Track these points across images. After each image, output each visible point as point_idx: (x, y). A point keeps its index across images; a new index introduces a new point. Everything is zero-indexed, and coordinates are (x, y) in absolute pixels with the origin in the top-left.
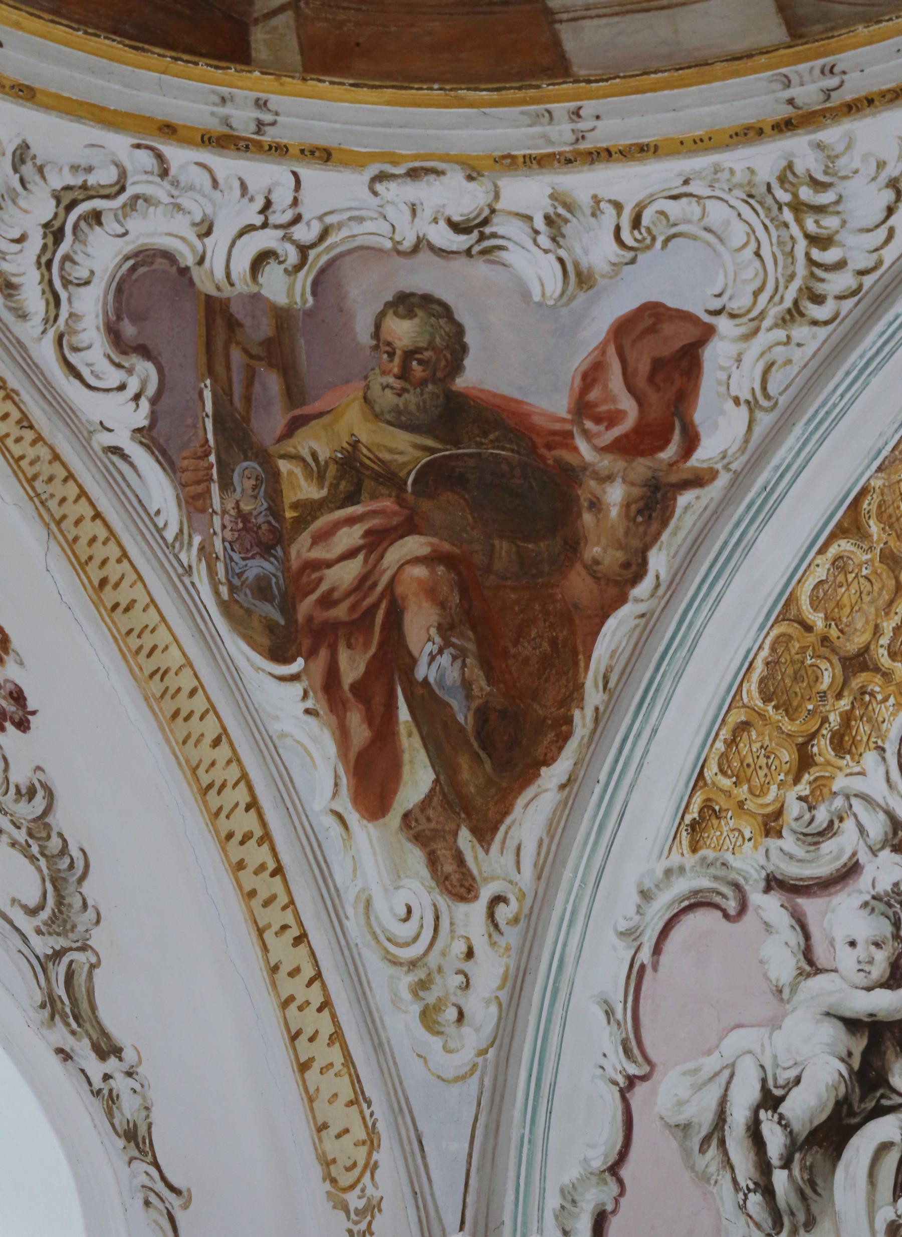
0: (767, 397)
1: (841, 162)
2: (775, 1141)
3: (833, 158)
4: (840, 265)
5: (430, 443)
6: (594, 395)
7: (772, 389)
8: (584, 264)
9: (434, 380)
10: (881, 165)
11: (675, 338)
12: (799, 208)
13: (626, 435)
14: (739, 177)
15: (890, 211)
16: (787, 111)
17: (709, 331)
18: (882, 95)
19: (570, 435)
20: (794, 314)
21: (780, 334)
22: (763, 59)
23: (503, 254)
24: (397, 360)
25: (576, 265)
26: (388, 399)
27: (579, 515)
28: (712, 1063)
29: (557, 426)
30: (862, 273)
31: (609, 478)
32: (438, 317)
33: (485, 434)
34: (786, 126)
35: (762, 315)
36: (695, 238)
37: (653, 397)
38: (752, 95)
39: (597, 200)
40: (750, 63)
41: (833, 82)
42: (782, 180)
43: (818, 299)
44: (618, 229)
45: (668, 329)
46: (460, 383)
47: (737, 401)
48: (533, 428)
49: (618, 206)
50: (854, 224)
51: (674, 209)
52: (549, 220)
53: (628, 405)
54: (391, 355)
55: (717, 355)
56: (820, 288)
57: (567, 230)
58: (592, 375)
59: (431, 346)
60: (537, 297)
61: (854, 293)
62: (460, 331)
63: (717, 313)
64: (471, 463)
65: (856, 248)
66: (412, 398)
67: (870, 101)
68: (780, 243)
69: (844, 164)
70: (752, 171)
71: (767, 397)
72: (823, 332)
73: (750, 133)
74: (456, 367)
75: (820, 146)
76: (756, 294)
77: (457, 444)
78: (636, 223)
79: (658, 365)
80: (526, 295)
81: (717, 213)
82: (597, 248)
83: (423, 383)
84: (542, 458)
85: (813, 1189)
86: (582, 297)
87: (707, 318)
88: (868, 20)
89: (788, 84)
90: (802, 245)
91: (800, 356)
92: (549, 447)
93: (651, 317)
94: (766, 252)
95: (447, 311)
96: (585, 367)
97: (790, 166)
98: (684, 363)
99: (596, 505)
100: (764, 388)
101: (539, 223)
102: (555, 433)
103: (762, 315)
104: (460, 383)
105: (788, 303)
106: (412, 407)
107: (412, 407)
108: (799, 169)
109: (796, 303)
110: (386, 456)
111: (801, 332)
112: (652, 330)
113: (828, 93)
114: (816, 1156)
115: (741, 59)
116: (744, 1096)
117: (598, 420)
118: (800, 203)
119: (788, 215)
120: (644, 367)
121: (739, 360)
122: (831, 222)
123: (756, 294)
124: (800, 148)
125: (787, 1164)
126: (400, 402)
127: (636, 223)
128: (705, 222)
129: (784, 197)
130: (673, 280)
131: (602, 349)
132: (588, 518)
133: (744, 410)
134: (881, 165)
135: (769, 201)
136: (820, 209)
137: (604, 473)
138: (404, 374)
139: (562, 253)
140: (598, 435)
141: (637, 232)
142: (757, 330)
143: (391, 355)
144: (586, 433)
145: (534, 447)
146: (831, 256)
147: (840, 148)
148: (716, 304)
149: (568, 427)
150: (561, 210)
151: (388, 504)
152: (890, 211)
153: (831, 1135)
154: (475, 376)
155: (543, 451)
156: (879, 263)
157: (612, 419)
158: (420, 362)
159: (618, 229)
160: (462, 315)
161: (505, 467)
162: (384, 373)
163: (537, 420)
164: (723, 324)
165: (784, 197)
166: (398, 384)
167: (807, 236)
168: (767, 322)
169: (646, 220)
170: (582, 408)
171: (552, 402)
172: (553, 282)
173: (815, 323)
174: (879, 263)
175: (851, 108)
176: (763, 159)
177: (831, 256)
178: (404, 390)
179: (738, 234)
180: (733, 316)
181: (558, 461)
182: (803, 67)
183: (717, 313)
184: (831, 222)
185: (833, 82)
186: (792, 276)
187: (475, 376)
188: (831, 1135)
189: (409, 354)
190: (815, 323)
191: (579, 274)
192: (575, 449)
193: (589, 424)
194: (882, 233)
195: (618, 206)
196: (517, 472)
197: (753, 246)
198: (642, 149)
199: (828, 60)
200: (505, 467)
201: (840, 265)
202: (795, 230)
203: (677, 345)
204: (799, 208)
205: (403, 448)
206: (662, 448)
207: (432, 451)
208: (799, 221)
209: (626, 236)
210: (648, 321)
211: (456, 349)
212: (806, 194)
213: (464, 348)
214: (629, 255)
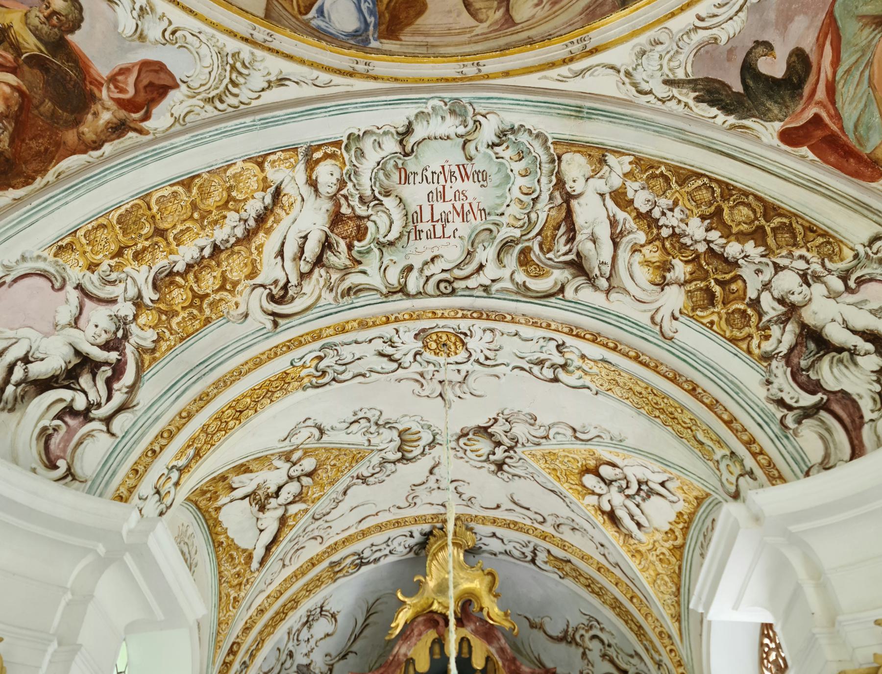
0: (184, 120)
1: (256, 63)
2: (18, 374)
3: (255, 61)
4: (236, 96)
5: (43, 49)
6: (120, 78)
7: (187, 119)
8: (145, 33)
9: (59, 28)
10: (269, 74)
11: (163, 80)
12: (233, 68)
13: (124, 100)
14: (218, 44)
15: (263, 90)
16: (248, 36)
17: (177, 86)
18: (283, 53)
19: (102, 85)
20: (211, 100)
21: (202, 104)
22: (251, 16)
23: (116, 6)
24: (49, 11)
25: (142, 31)
26: (36, 22)
27: (87, 114)
28: (10, 333)
29: (99, 79)
30: (241, 103)
31: (108, 109)
32: (76, 8)
33: (68, 62)
34: (246, 40)
35: (199, 93)
36: (191, 53)
37: (142, 94)
38: (242, 25)
39: (164, 15)
40: (246, 14)
41: (269, 39)
42: (233, 55)
43: (222, 101)
44: (165, 30)
45: (162, 75)
46: (69, 37)
47: (172, 115)
48: (89, 72)
49: (170, 23)
50: (249, 86)
51: (190, 38)
52: (141, 8)
53: (131, 91)
54: (47, 7)
55: (174, 96)
56: (224, 98)
57: (146, 16)
58: (124, 71)
59: (66, 16)
60: (120, 30)
61: (235, 107)
62: (82, 19)
63: (184, 82)
64: (56, 67)
65: (245, 94)
66: (46, 28)
67: (278, 52)
68: (220, 75)
69: (257, 65)
70: (225, 45)
71: (184, 120)
72: (216, 113)
73: (233, 34)
74: (72, 31)
75: (252, 54)
76: (201, 85)
77: (53, 57)
78: (174, 33)
79: (151, 84)
80: (116, 27)
81: (204, 50)
82: (154, 31)
83: (54, 26)
84: (86, 85)
85: (21, 400)
86: (137, 43)
87: (179, 81)
88: (292, 30)
89: (254, 29)
90: (227, 80)
91: (203, 115)
92: (91, 83)
93: (159, 67)
94: (213, 74)
95: (81, 9)
96: (123, 66)
97: (239, 53)
98: (161, 90)
99: (96, 114)
100: (184, 117)
101: (137, 7)
102: (96, 80)
103: (199, 93)
104: (69, 37)
105: (210, 96)
106: (44, 32)
107: (44, 32)
108: (241, 56)
109: (213, 97)
110: (21, 40)
111: (209, 107)
112: (156, 71)
113: (265, 41)
114: (31, 389)
115: (243, 11)
116: (16, 352)
117: (116, 87)
118: (236, 68)
119: (228, 68)
120: (145, 82)
121: (181, 102)
122: (241, 80)
123: (201, 85)
124: (246, 50)
125: (17, 385)
126: (40, 26)
127: (174, 33)
128: (198, 50)
129: (231, 61)
130: (176, 62)
131: (134, 65)
132: (90, 117)
133: (173, 119)
134: (269, 74)
135: (225, 59)
136: (240, 73)
137: (106, 106)
138: (48, 18)
139: (139, 23)
140: (113, 92)
141: (171, 36)
142: (194, 97)
143: (47, 7)
144: (108, 88)
145: (85, 79)
146: (235, 90)
147: (258, 59)
148: (185, 79)
149: (103, 82)
150: (148, 8)
151: (10, 57)
152: (263, 90)
153: (43, 385)
154: (75, 39)
155: (88, 83)
156: (249, 104)
157: (122, 91)
158: (58, 18)
159: (165, 30)
160: (86, 14)
161: (68, 78)
162: (40, 11)
163: (92, 71)
164: (183, 87)
165: (231, 61)
166: (43, 19)
167: (231, 79)
168: (199, 97)
169: (178, 34)
170: (113, 79)
171: (102, 68)
172: (129, 30)
173: (216, 108)
174: (249, 104)
175: (270, 50)
176: (232, 45)
177: (235, 90)
178: (44, 23)
179: (207, 62)
180: (188, 87)
181: (91, 92)
182: (263, 29)
183: (184, 82)
184: (241, 80)
185: (269, 39)
186: (217, 88)
187: (75, 39)
188: (43, 385)
189: (55, 13)
190: (216, 108)
191: (141, 34)
192: (101, 91)
193: (112, 86)
194: (257, 95)
195: (170, 23)
196: (72, 83)
197: (210, 69)
198: (191, 11)
199: (272, 32)
200: (68, 78)
201: (236, 96)
202: (228, 74)
203: (162, 82)
204: (233, 68)
205: (31, 44)
206: (134, 112)
207: (42, 51)
208: (231, 72)
209: (167, 34)
210: (157, 68)
211: (76, 24)
212: (238, 65)
213: (79, 27)
214: (164, 41)
